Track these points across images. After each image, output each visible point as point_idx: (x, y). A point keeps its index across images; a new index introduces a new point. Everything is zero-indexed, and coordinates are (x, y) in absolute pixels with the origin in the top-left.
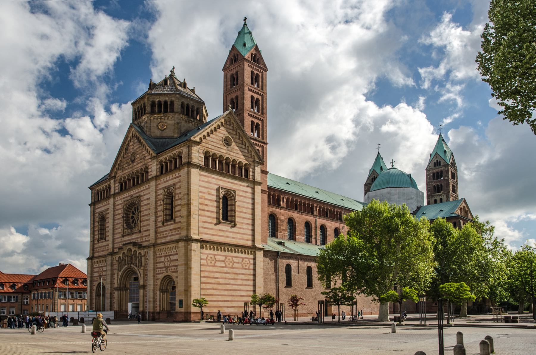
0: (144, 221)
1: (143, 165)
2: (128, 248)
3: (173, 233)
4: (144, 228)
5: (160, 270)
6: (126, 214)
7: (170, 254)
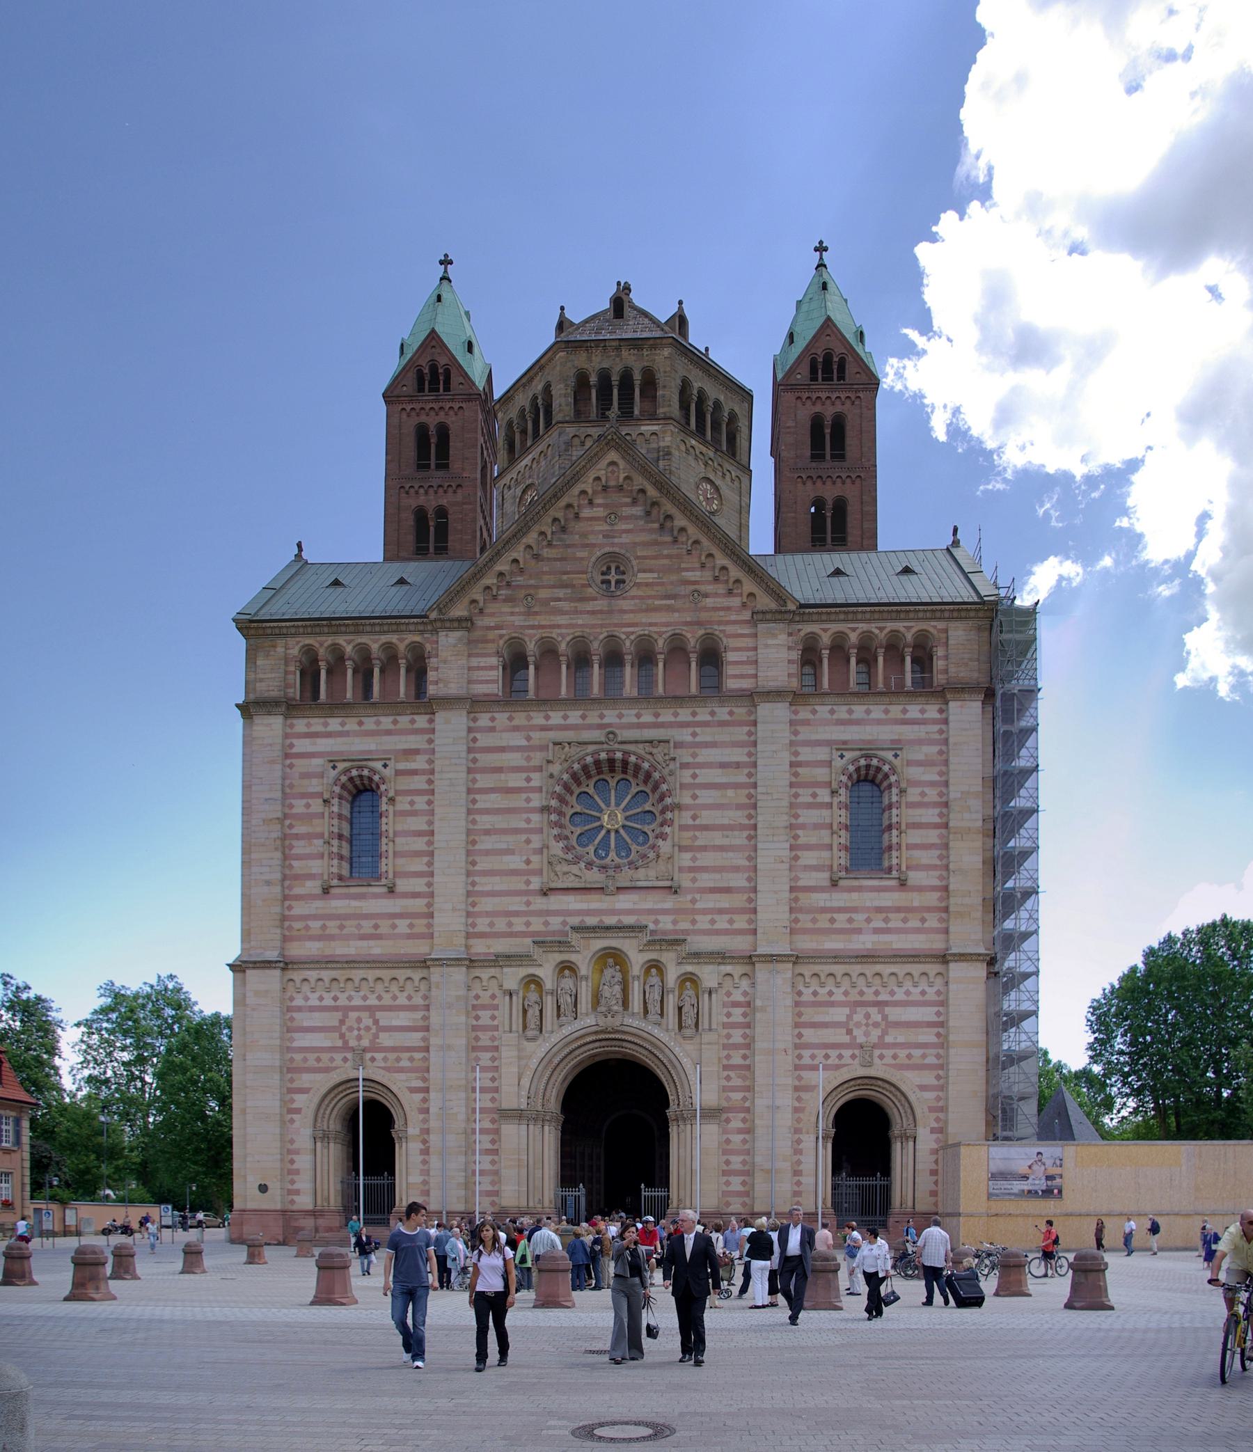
0: (704, 848)
2: (598, 944)
3: (895, 923)
4: (705, 876)
5: (820, 1053)
6: (562, 800)
7: (884, 997)
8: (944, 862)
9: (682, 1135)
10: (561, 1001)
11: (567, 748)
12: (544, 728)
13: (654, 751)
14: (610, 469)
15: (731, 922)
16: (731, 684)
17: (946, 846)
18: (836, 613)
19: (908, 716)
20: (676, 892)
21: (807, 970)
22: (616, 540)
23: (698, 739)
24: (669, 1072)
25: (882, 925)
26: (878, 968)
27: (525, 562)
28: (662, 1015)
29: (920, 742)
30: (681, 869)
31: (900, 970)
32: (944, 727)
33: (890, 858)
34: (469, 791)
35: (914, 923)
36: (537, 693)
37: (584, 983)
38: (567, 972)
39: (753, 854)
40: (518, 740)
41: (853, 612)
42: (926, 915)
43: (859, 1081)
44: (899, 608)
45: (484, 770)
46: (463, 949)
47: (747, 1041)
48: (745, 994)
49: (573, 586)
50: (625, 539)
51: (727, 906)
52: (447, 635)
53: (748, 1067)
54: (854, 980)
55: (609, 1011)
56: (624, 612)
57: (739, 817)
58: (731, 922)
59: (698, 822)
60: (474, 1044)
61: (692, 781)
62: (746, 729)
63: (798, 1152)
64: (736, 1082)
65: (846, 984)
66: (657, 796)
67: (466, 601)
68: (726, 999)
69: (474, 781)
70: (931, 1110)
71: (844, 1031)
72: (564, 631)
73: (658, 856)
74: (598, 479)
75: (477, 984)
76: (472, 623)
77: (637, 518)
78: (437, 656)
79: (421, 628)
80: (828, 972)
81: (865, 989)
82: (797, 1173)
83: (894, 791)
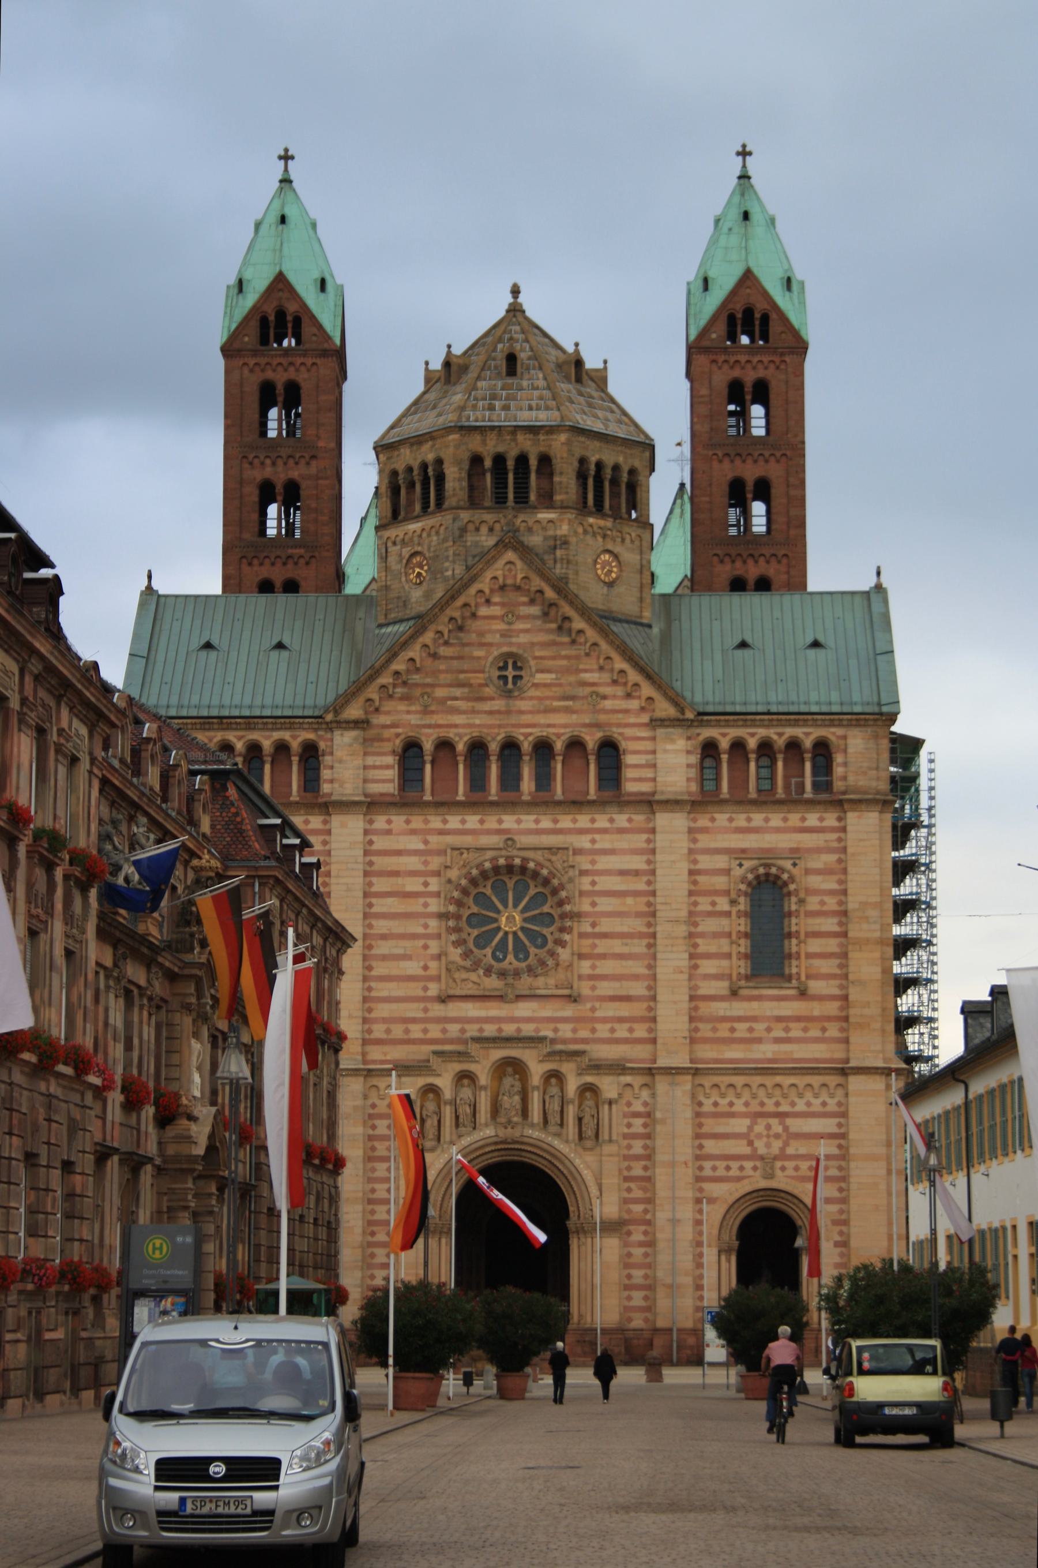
0: (603, 956)
1: (585, 725)
2: (498, 1054)
3: (796, 1032)
4: (605, 984)
5: (721, 1164)
6: (459, 904)
7: (785, 1108)
8: (844, 971)
9: (583, 1248)
10: (460, 1111)
11: (465, 855)
12: (441, 832)
13: (554, 858)
14: (508, 566)
15: (631, 1030)
16: (630, 787)
17: (845, 955)
18: (734, 720)
19: (807, 824)
20: (575, 1001)
21: (707, 1081)
22: (514, 640)
23: (597, 846)
24: (569, 1183)
25: (782, 1034)
26: (778, 1079)
27: (422, 660)
28: (562, 1125)
29: (819, 850)
30: (580, 977)
31: (800, 1081)
32: (842, 835)
33: (790, 966)
34: (366, 895)
35: (814, 1033)
36: (432, 794)
37: (483, 1093)
38: (466, 1081)
39: (652, 962)
40: (415, 843)
41: (752, 720)
42: (826, 1024)
43: (761, 1193)
44: (797, 717)
45: (381, 874)
46: (360, 1057)
47: (648, 1152)
48: (645, 1104)
49: (470, 685)
50: (523, 639)
51: (625, 1013)
52: (342, 735)
53: (648, 1179)
54: (754, 1091)
55: (509, 1122)
56: (521, 712)
57: (638, 925)
58: (631, 1030)
59: (597, 930)
60: (371, 1154)
61: (589, 888)
62: (645, 836)
63: (699, 1265)
64: (637, 1194)
65: (746, 1095)
66: (556, 899)
67: (361, 700)
68: (626, 1109)
69: (370, 884)
70: (836, 1223)
71: (745, 1142)
72: (461, 731)
73: (557, 965)
74: (495, 578)
75: (373, 1094)
76: (367, 722)
77: (535, 617)
78: (332, 754)
79: (316, 726)
80: (728, 1083)
81: (766, 1100)
82: (699, 1287)
83: (794, 899)
